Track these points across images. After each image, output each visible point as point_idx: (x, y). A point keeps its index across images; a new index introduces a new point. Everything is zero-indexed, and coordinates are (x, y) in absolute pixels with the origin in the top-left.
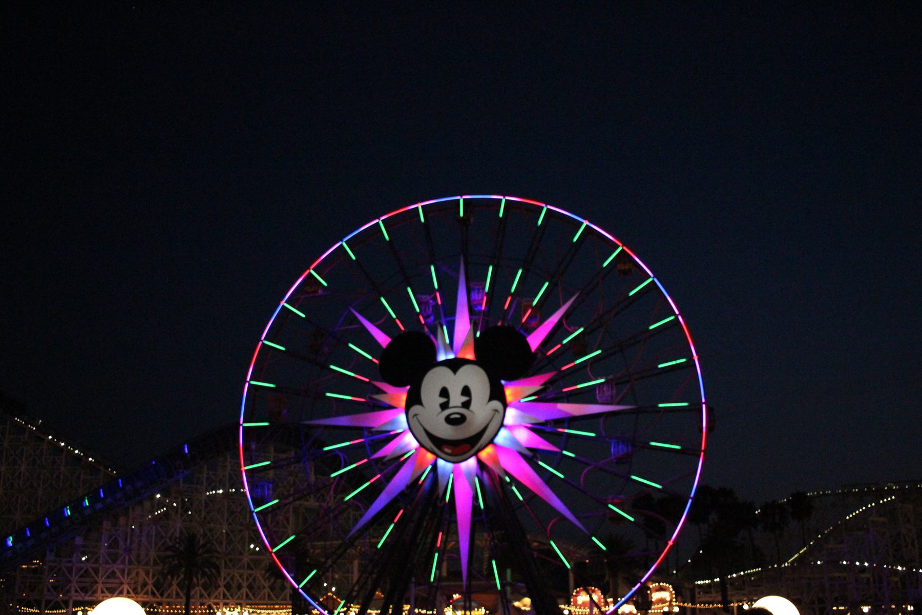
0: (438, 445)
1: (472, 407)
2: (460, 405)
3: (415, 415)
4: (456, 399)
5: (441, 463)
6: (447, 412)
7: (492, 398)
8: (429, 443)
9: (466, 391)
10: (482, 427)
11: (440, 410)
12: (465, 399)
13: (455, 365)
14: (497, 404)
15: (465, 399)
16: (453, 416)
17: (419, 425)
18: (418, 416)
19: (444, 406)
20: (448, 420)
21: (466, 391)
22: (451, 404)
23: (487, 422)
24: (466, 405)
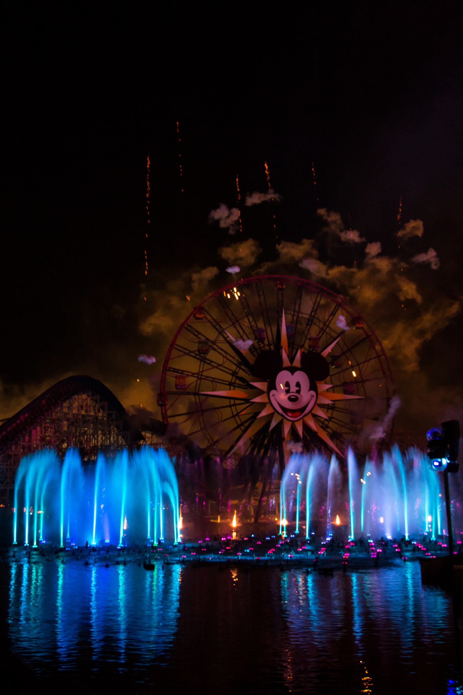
0: (285, 410)
2: (295, 392)
3: (273, 395)
4: (293, 388)
5: (285, 420)
6: (289, 395)
7: (310, 389)
8: (280, 410)
9: (298, 385)
10: (307, 403)
12: (298, 388)
13: (292, 370)
14: (313, 393)
15: (298, 388)
17: (275, 401)
18: (275, 396)
19: (287, 391)
20: (290, 399)
21: (298, 385)
22: (291, 391)
23: (308, 401)
24: (298, 392)
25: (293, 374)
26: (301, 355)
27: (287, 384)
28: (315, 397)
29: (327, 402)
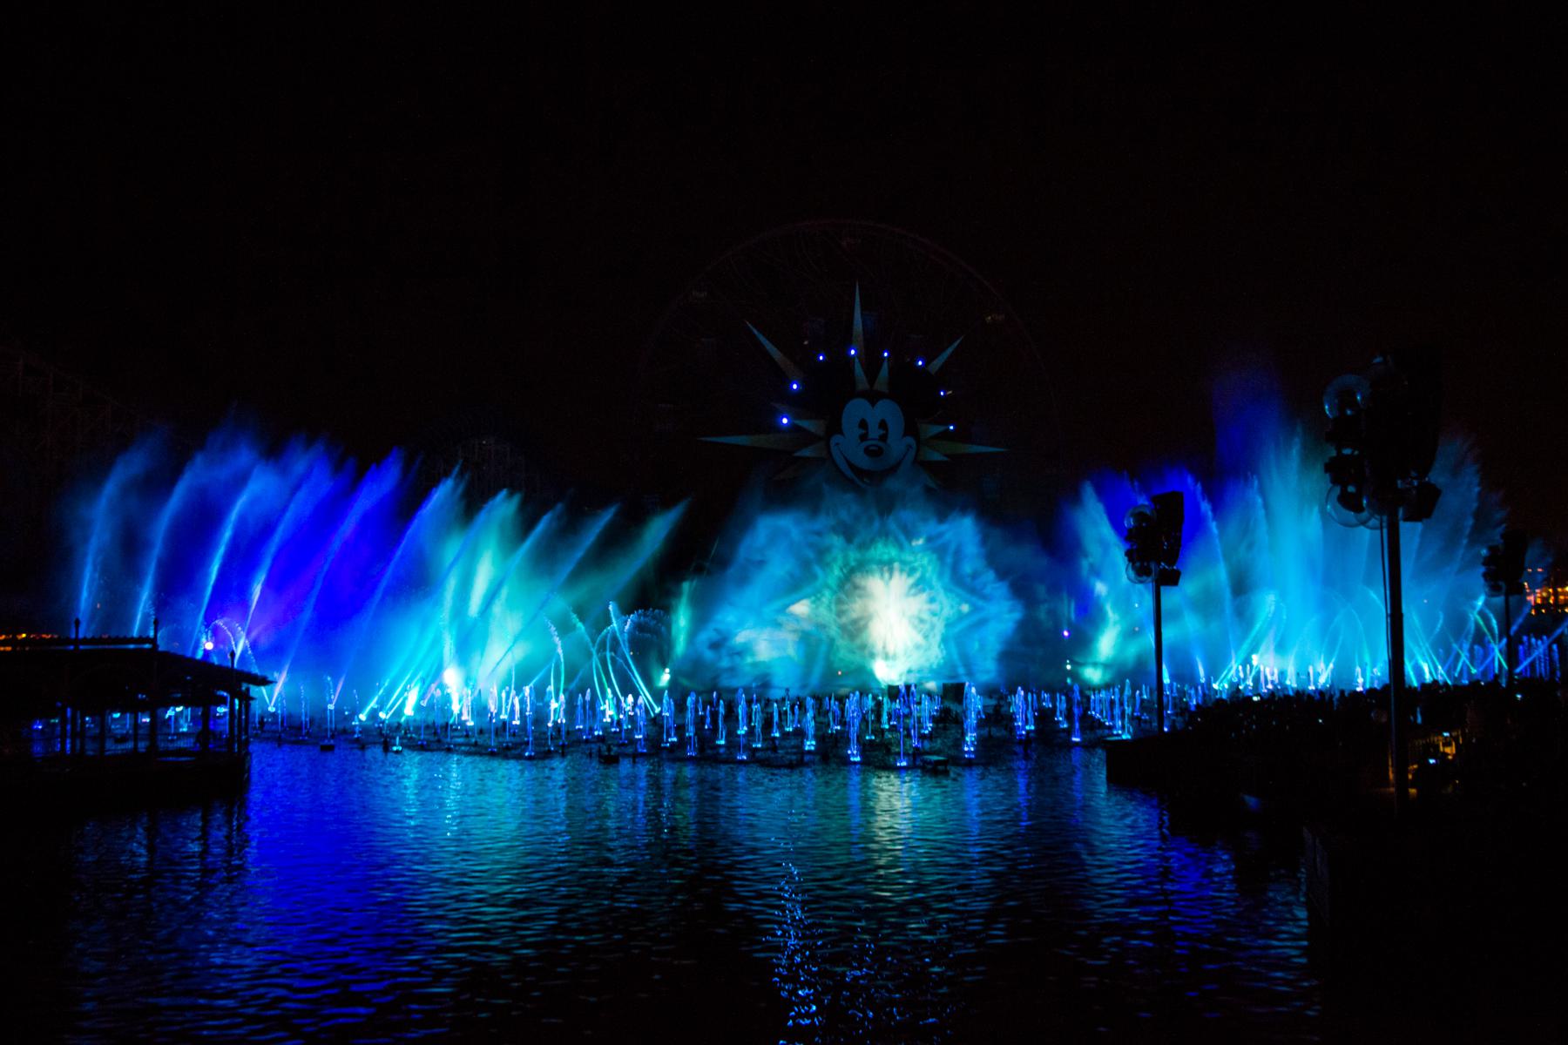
1: (889, 441)
2: (877, 437)
3: (837, 444)
4: (874, 432)
7: (906, 434)
8: (849, 473)
9: (883, 425)
11: (859, 441)
12: (882, 432)
13: (873, 397)
14: (910, 440)
15: (882, 432)
16: (872, 448)
19: (863, 438)
20: (867, 451)
21: (883, 425)
24: (884, 438)
25: (873, 404)
26: (891, 370)
27: (863, 424)
28: (914, 446)
29: (937, 457)
